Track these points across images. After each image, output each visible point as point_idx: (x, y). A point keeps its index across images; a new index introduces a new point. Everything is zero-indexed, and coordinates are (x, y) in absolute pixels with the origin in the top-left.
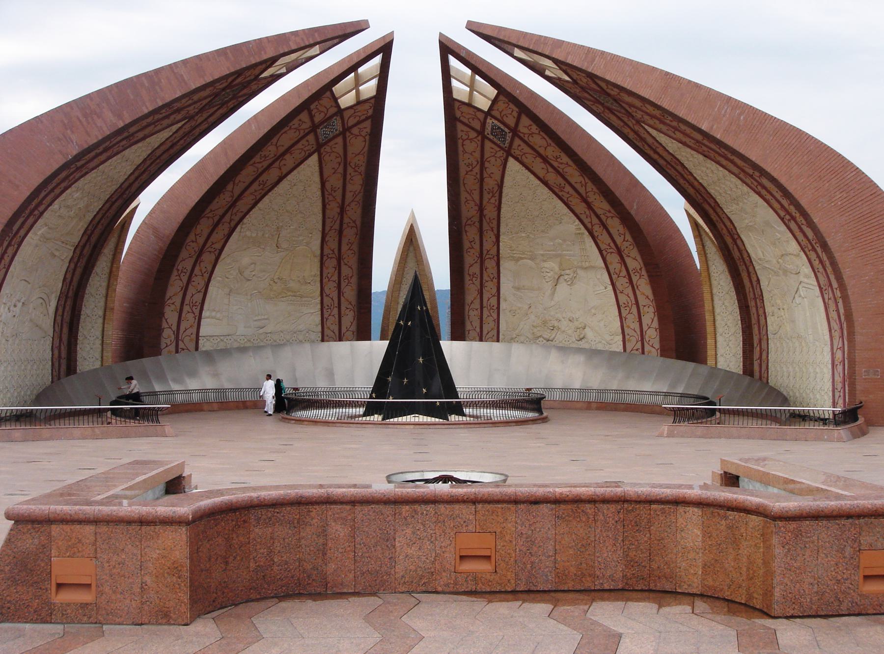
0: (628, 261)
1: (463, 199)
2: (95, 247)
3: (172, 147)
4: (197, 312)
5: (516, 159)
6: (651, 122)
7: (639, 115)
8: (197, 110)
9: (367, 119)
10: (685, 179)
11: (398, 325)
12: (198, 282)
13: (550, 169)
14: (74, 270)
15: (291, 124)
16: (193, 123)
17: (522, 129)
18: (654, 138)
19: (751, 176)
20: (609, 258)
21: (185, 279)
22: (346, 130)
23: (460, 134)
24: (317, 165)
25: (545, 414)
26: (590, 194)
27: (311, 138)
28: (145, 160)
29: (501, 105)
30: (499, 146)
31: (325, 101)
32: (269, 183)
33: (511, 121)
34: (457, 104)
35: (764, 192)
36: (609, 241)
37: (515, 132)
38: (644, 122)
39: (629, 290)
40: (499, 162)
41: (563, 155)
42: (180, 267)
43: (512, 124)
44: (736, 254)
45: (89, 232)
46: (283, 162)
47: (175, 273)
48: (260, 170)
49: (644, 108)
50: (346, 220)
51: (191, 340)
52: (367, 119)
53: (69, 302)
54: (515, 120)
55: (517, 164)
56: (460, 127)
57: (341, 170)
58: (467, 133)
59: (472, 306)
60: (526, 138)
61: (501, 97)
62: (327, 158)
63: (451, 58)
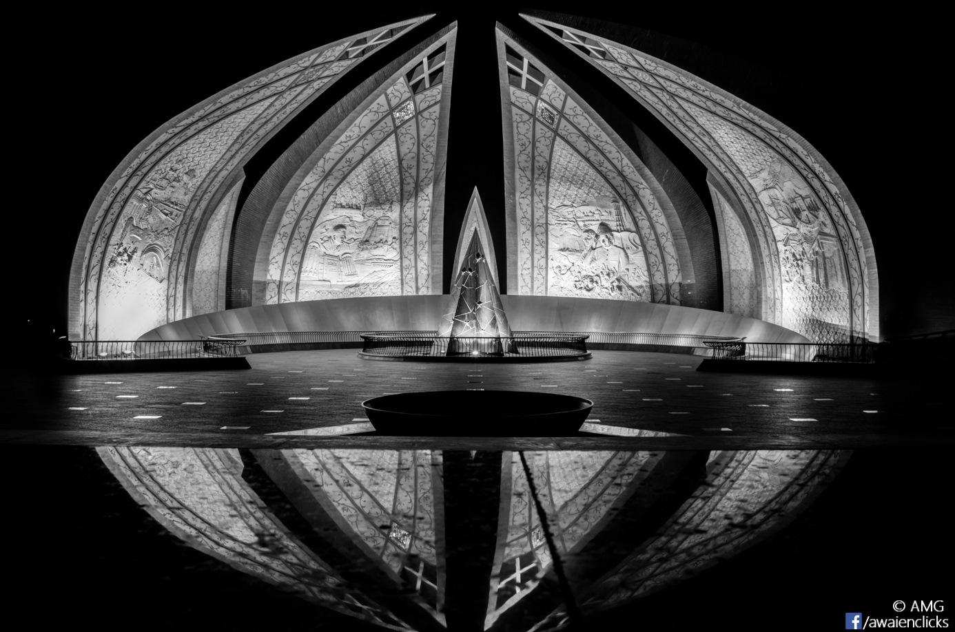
0: (658, 227)
1: (517, 176)
2: (205, 212)
3: (266, 123)
4: (297, 270)
5: (563, 138)
6: (685, 94)
7: (673, 88)
8: (284, 88)
9: (436, 103)
10: (710, 149)
11: (460, 274)
12: (297, 244)
14: (187, 231)
15: (370, 108)
16: (284, 102)
18: (686, 111)
19: (778, 139)
20: (640, 223)
21: (286, 242)
22: (418, 113)
23: (515, 117)
24: (395, 145)
25: (589, 352)
26: (626, 169)
28: (241, 135)
30: (548, 127)
32: (354, 161)
33: (559, 104)
35: (787, 153)
36: (640, 209)
37: (561, 113)
38: (677, 96)
39: (657, 251)
40: (548, 142)
41: (603, 134)
42: (282, 232)
43: (560, 108)
44: (753, 216)
45: (198, 198)
46: (366, 142)
47: (278, 237)
48: (347, 149)
49: (678, 81)
50: (421, 194)
51: (291, 293)
52: (436, 103)
53: (184, 258)
55: (563, 142)
58: (521, 118)
59: (525, 266)
60: (571, 120)
62: (402, 139)
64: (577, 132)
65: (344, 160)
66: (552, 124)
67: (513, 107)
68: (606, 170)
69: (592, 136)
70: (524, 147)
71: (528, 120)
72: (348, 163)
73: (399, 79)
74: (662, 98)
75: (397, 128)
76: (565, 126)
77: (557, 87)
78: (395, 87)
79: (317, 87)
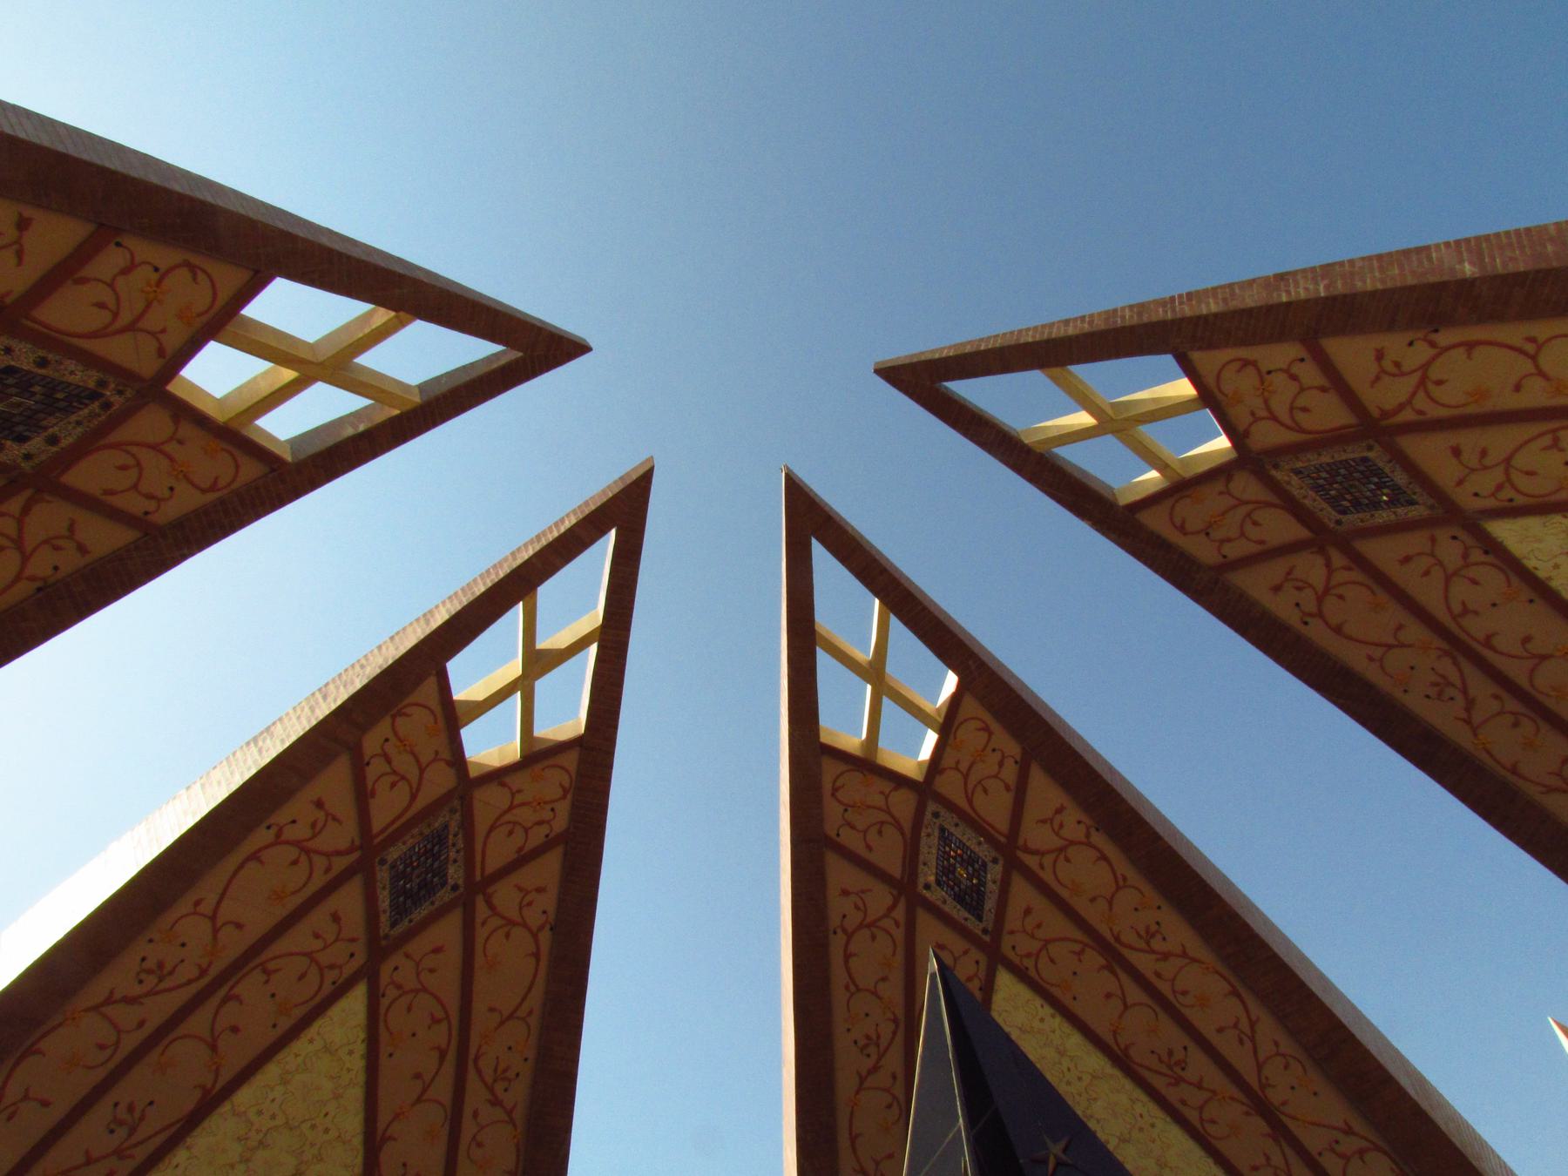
5: (1021, 974)
13: (1135, 994)
15: (282, 817)
17: (1035, 835)
23: (838, 907)
27: (349, 900)
29: (969, 735)
31: (416, 723)
33: (995, 808)
34: (830, 769)
37: (1009, 847)
48: (130, 1043)
54: (1007, 799)
56: (839, 874)
57: (443, 1089)
60: (1047, 876)
61: (970, 706)
63: (818, 550)
64: (1077, 934)
65: (102, 1112)
66: (976, 910)
67: (833, 862)
68: (1206, 1095)
69: (1129, 937)
70: (872, 1050)
71: (885, 916)
72: (122, 1132)
73: (421, 679)
74: (1429, 594)
75: (378, 950)
76: (1028, 911)
77: (995, 726)
78: (400, 721)
79: (41, 565)
